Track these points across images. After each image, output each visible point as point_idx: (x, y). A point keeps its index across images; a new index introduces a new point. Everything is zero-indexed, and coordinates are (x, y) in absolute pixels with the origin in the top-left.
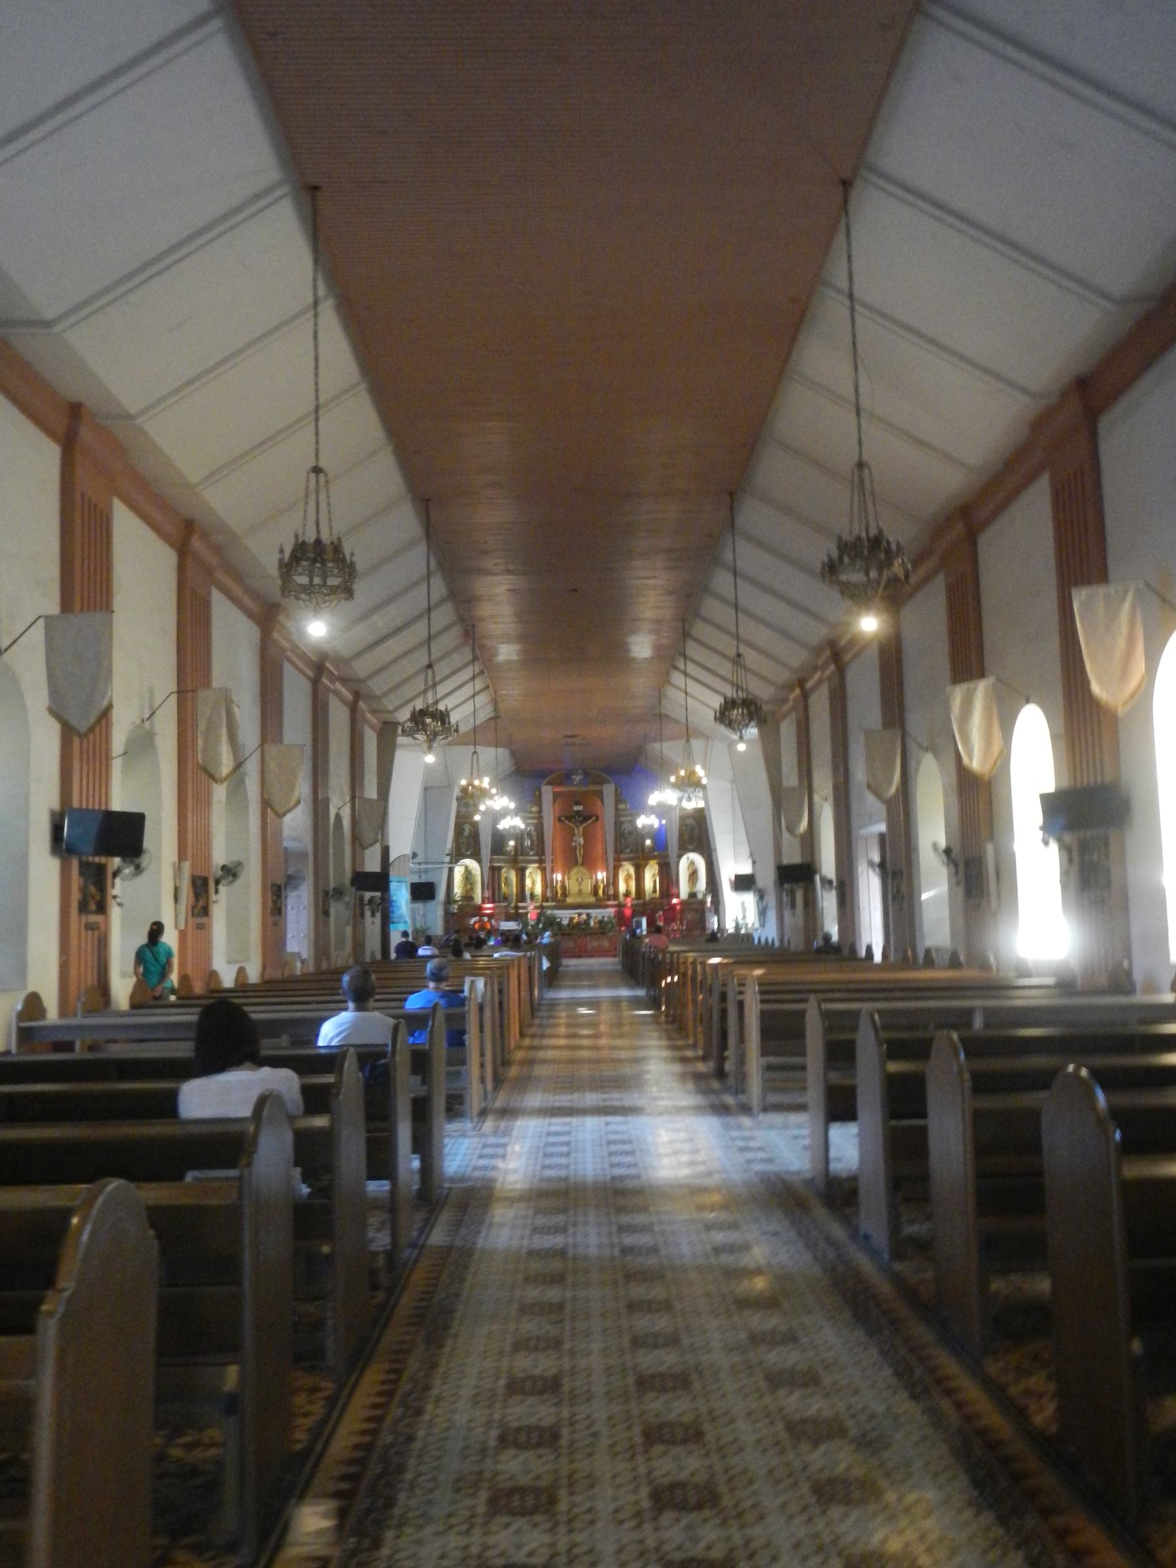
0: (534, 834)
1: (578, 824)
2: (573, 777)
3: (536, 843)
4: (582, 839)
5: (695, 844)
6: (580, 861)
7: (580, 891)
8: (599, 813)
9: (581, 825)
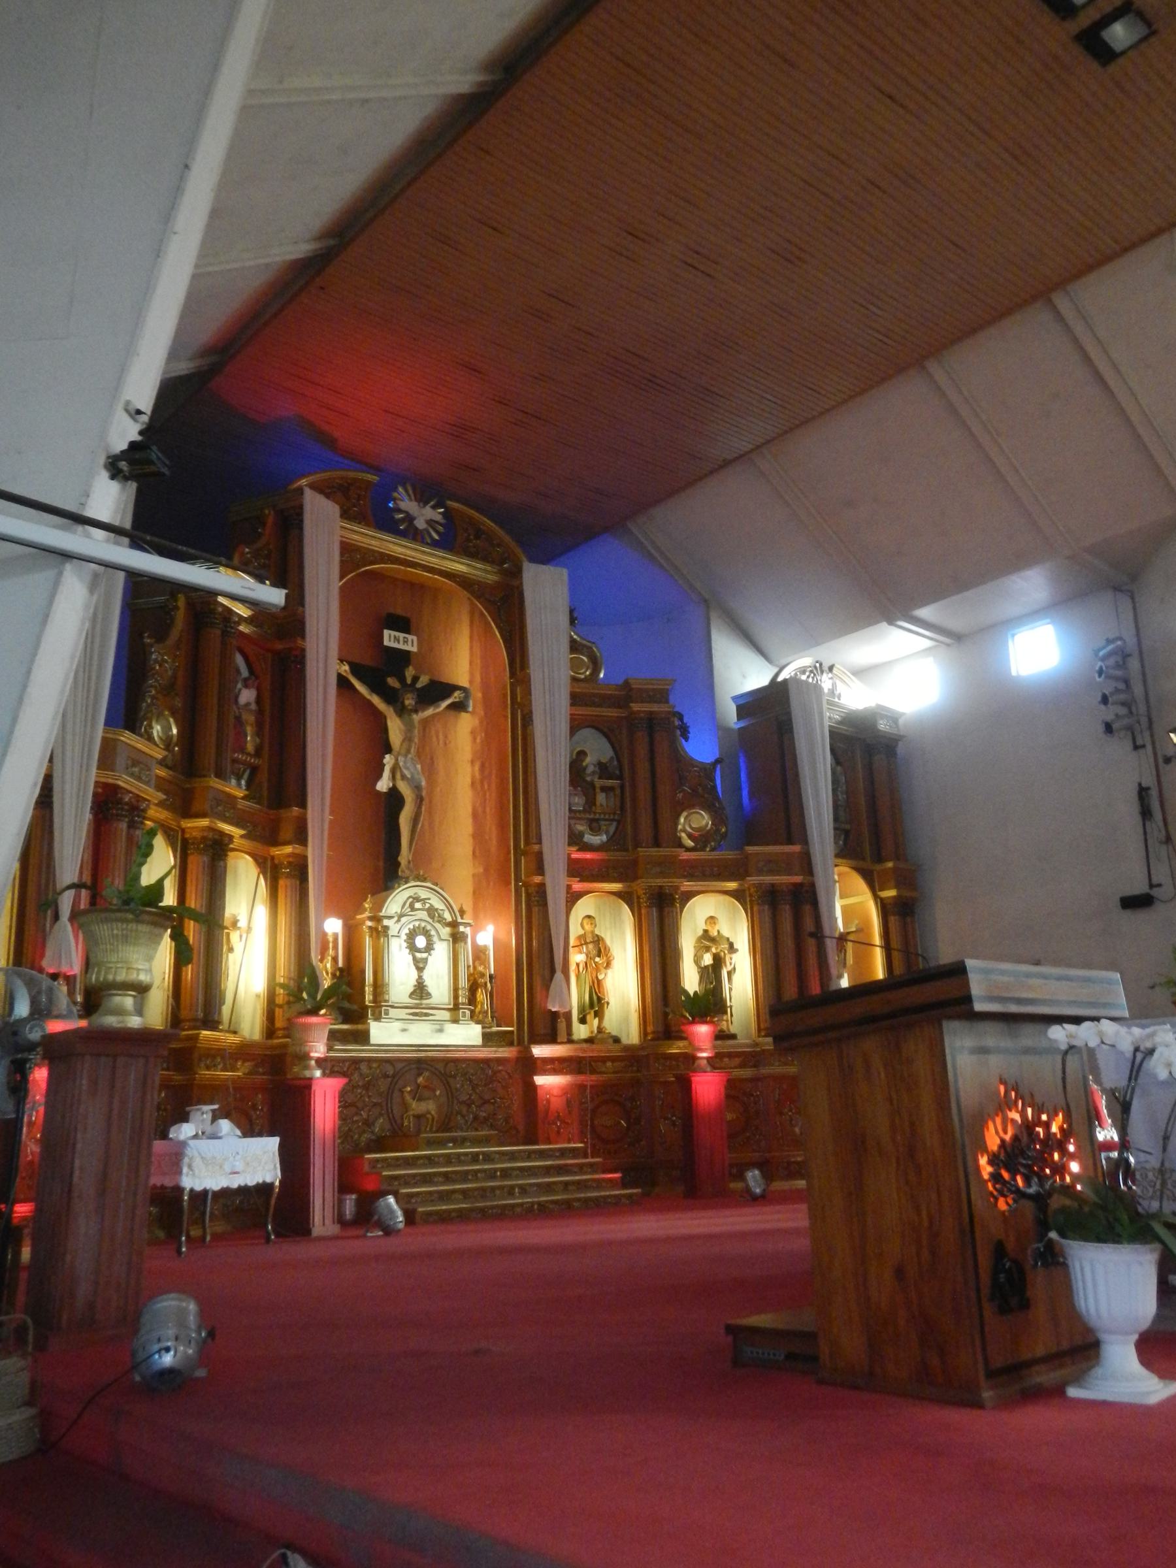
1: (409, 701)
4: (419, 767)
6: (404, 856)
7: (420, 990)
8: (463, 681)
9: (416, 711)
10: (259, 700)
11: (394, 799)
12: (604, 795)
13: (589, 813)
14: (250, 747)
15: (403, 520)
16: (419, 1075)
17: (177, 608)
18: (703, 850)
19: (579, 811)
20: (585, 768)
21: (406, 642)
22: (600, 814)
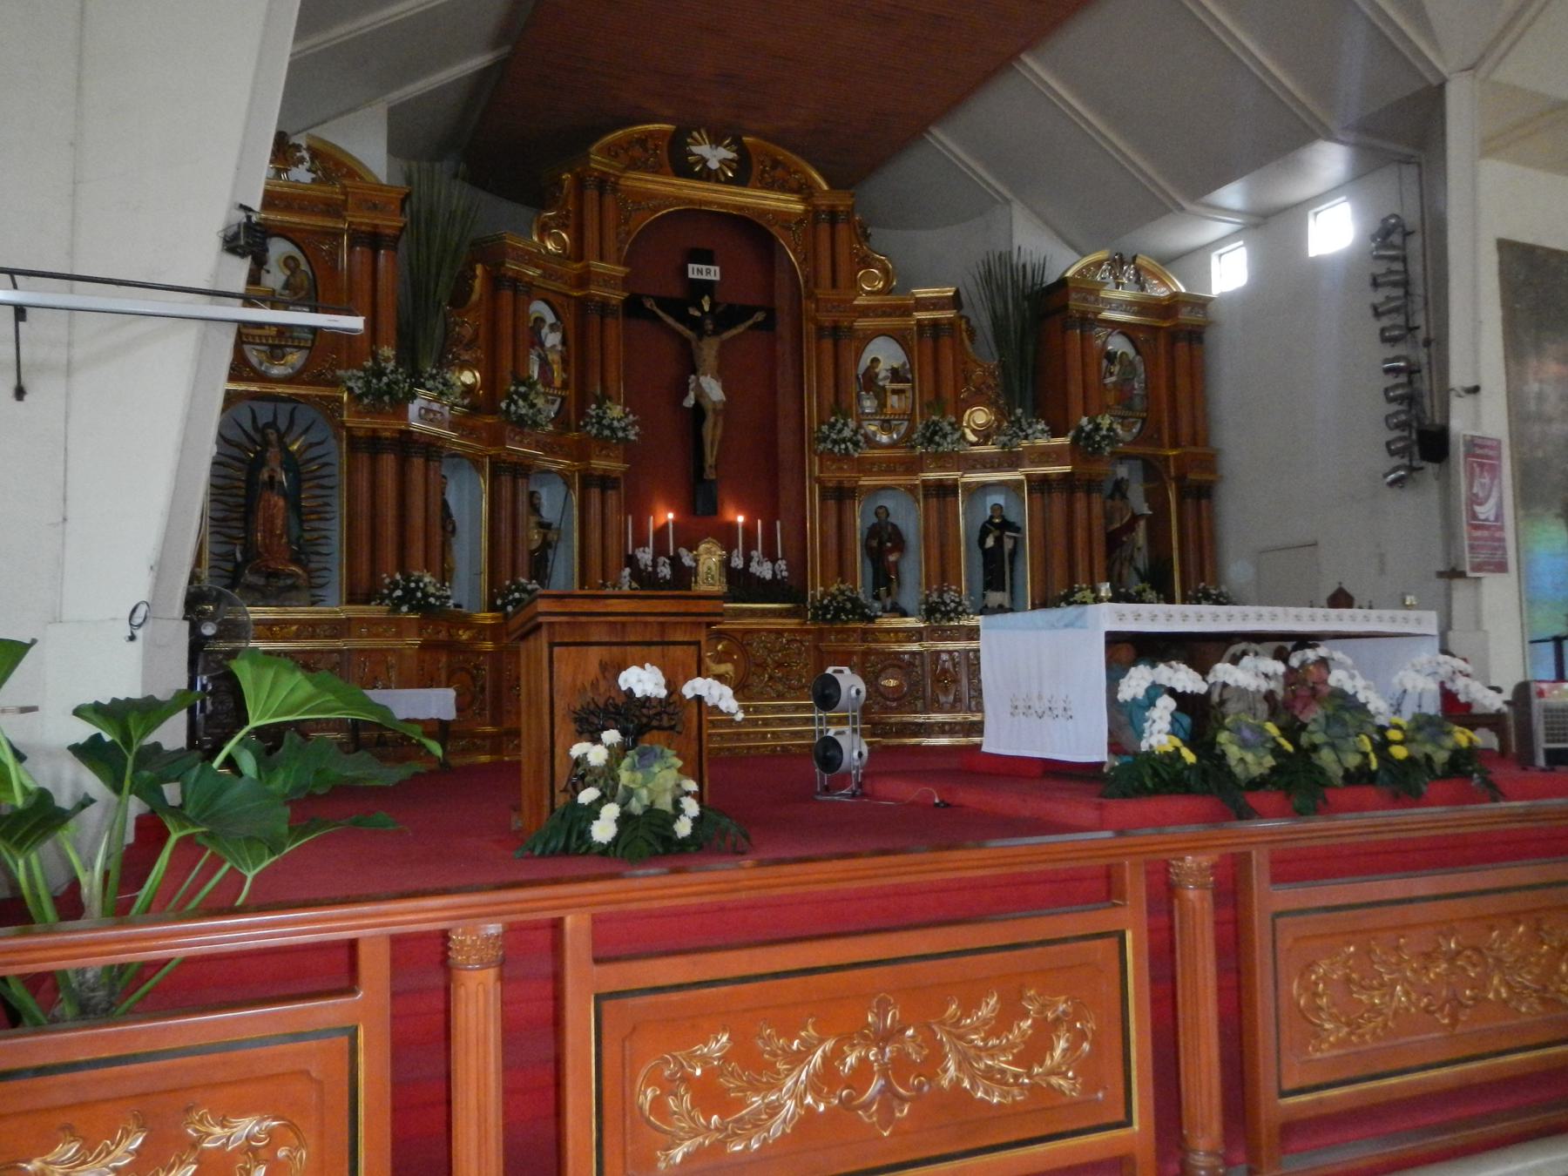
0: (552, 339)
1: (709, 325)
2: (695, 149)
3: (558, 376)
5: (1138, 426)
9: (716, 333)
10: (564, 342)
11: (699, 411)
12: (895, 398)
13: (881, 415)
14: (558, 382)
15: (696, 163)
16: (719, 643)
17: (474, 277)
18: (985, 443)
19: (868, 414)
20: (877, 375)
21: (708, 272)
22: (891, 415)
